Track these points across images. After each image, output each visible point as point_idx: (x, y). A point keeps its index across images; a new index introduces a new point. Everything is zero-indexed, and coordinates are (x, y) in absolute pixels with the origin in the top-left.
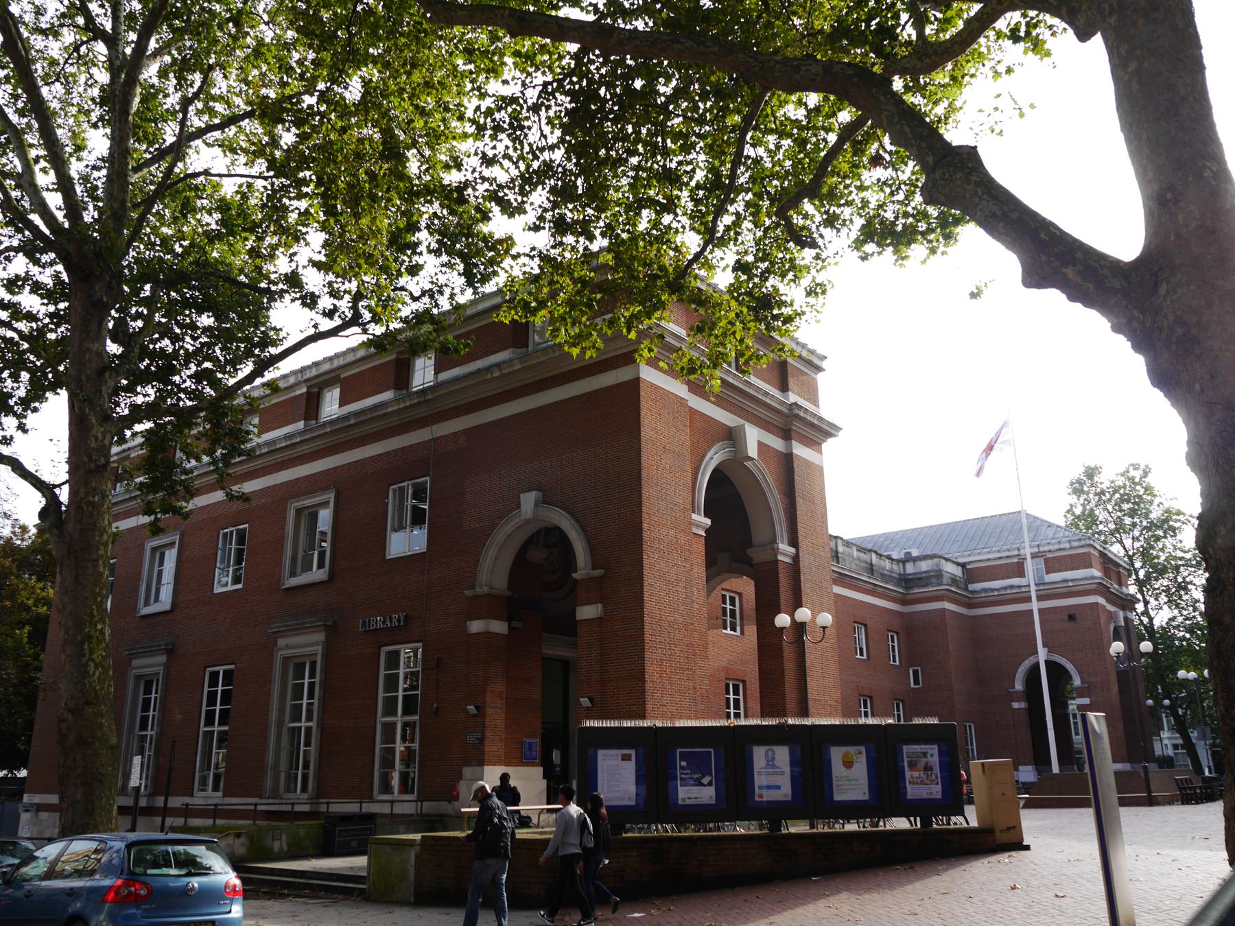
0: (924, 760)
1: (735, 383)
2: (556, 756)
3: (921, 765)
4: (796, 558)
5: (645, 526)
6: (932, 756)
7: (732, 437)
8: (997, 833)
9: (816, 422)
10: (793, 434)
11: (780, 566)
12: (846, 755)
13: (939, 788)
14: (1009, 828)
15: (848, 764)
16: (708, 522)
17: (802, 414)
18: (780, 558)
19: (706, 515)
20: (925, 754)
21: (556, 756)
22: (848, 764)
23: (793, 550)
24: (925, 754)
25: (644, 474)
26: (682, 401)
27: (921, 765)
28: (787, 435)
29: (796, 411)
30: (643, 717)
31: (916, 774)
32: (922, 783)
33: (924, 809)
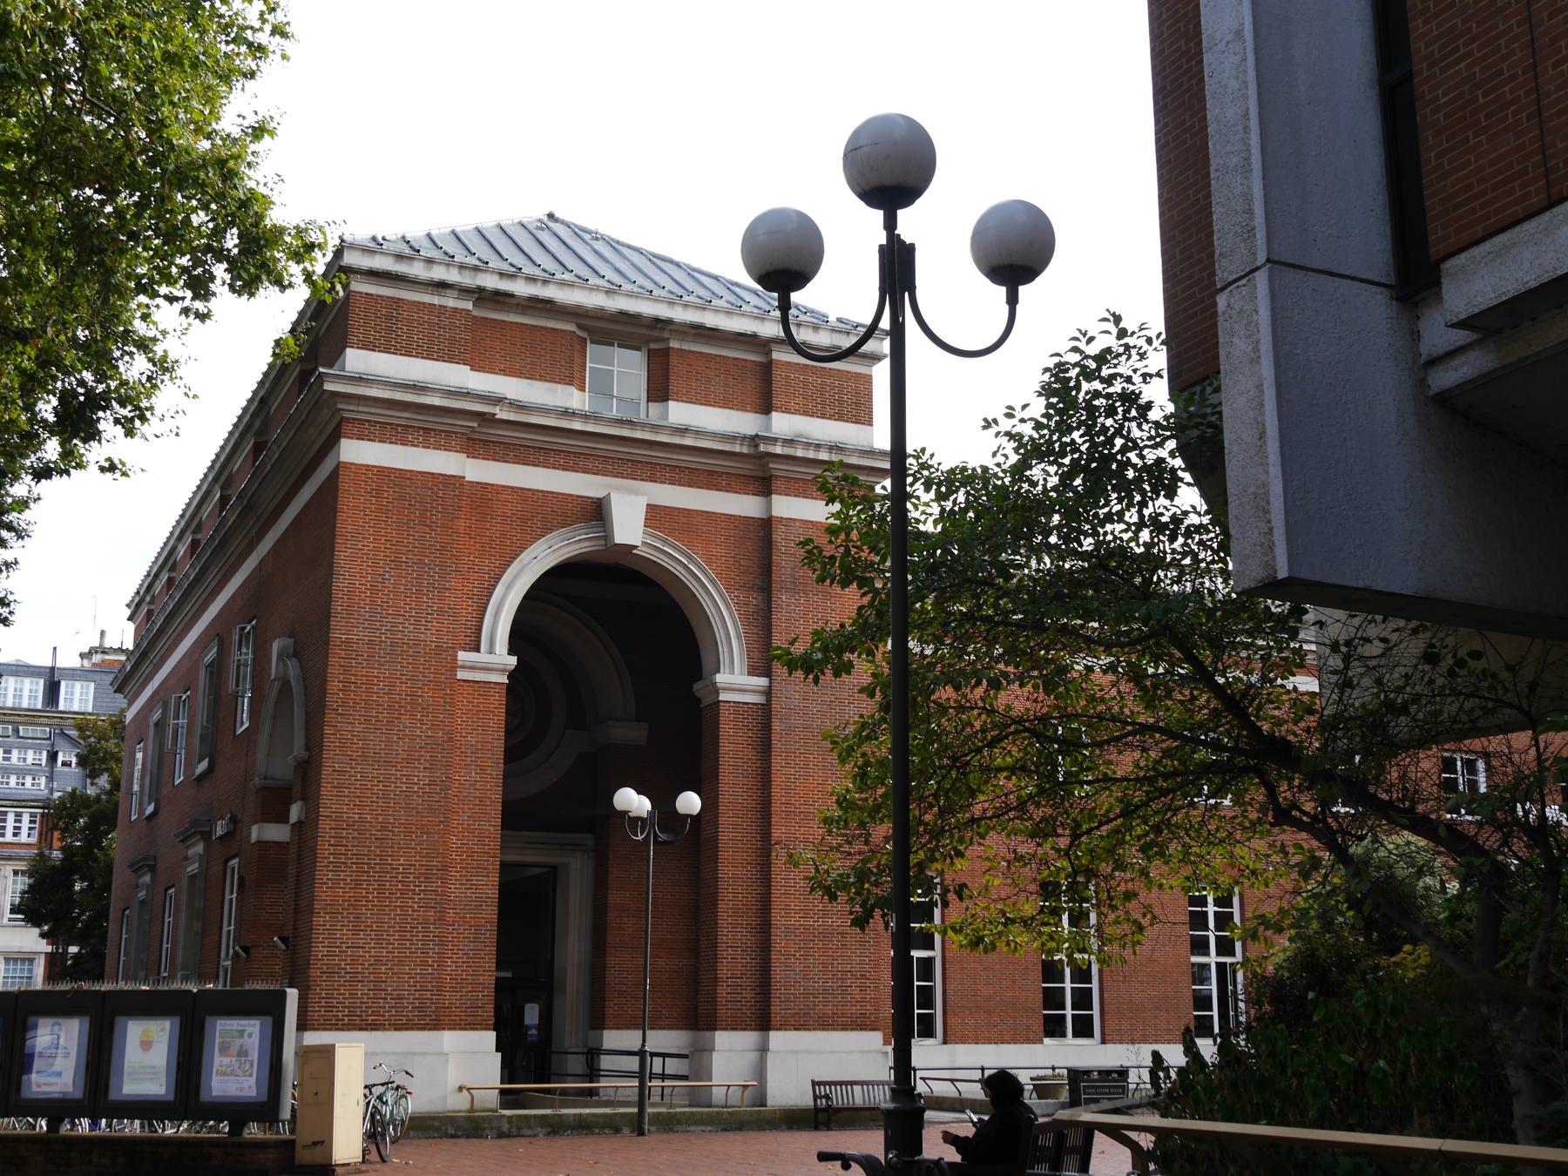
0: (239, 1042)
1: (590, 428)
2: (532, 1014)
3: (234, 1050)
4: (768, 693)
5: (334, 685)
6: (250, 1035)
7: (596, 512)
8: (298, 1148)
9: (824, 456)
10: (776, 484)
11: (725, 715)
12: (145, 1032)
13: (253, 1080)
14: (315, 1144)
15: (146, 1045)
16: (513, 660)
17: (778, 450)
18: (722, 697)
19: (510, 653)
20: (241, 1033)
21: (532, 1014)
22: (146, 1045)
23: (762, 682)
24: (241, 1033)
25: (337, 607)
26: (456, 482)
27: (234, 1050)
28: (764, 485)
29: (762, 448)
30: (100, 977)
31: (226, 1060)
32: (232, 1073)
33: (238, 1112)
